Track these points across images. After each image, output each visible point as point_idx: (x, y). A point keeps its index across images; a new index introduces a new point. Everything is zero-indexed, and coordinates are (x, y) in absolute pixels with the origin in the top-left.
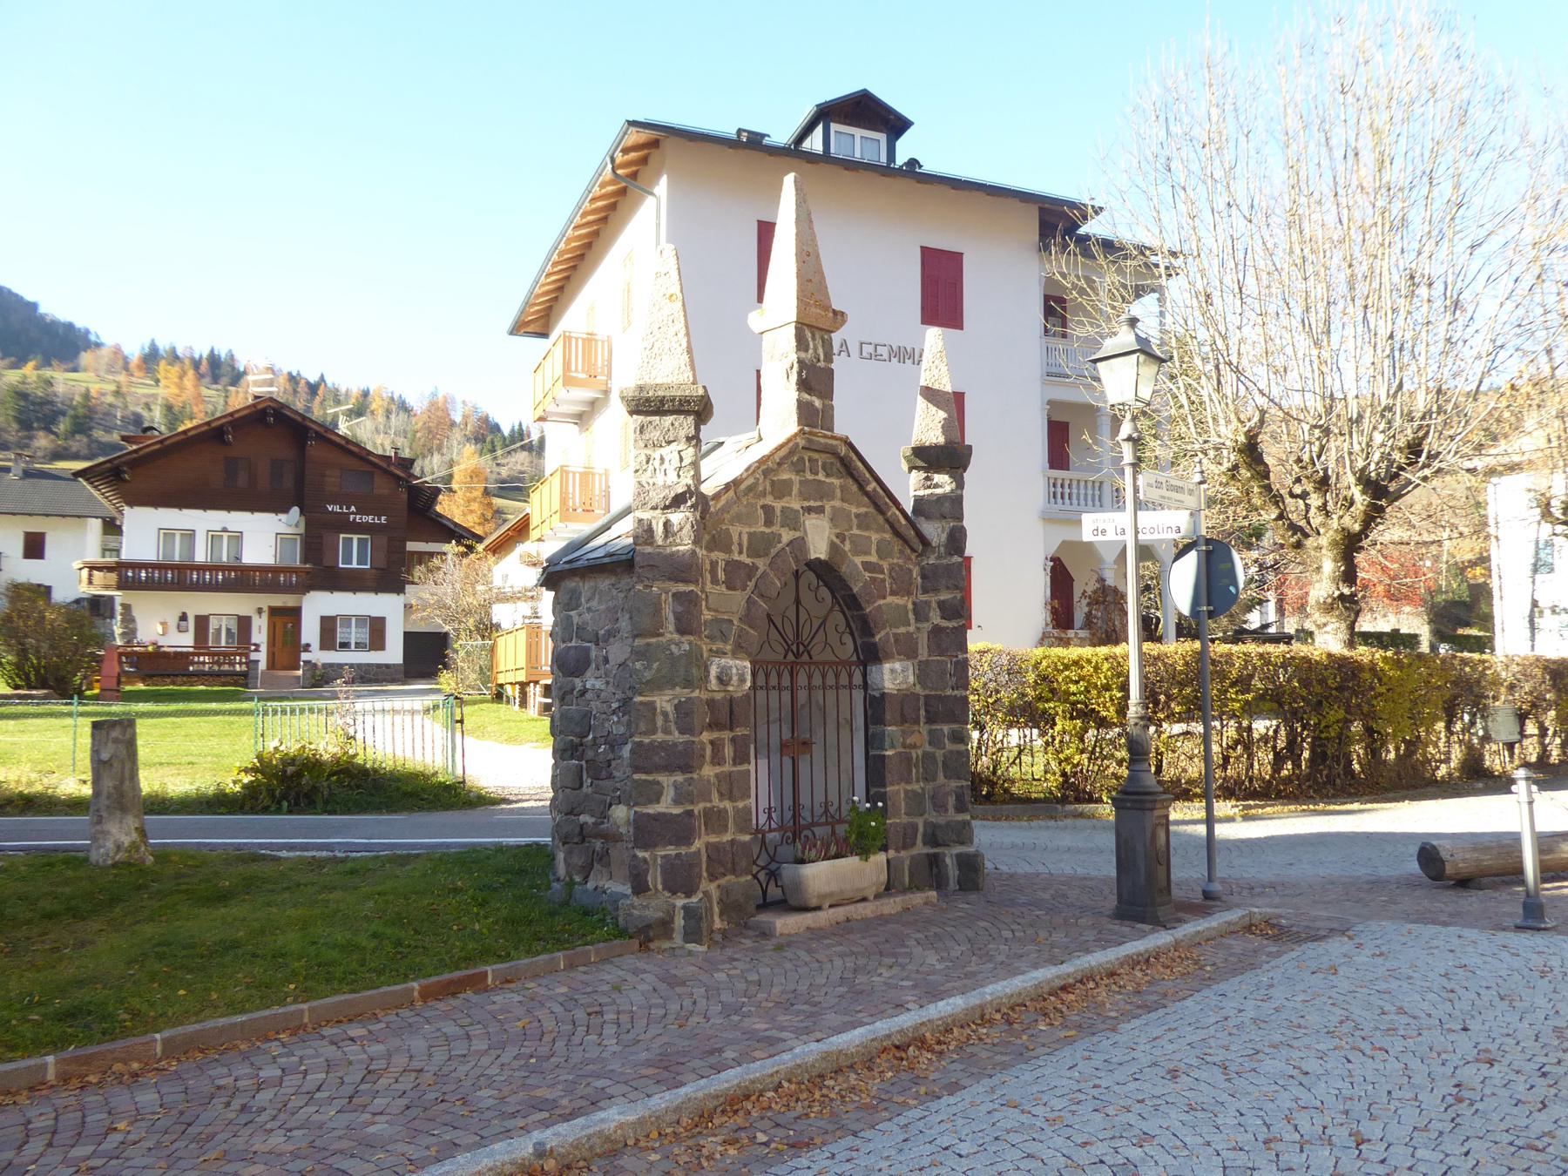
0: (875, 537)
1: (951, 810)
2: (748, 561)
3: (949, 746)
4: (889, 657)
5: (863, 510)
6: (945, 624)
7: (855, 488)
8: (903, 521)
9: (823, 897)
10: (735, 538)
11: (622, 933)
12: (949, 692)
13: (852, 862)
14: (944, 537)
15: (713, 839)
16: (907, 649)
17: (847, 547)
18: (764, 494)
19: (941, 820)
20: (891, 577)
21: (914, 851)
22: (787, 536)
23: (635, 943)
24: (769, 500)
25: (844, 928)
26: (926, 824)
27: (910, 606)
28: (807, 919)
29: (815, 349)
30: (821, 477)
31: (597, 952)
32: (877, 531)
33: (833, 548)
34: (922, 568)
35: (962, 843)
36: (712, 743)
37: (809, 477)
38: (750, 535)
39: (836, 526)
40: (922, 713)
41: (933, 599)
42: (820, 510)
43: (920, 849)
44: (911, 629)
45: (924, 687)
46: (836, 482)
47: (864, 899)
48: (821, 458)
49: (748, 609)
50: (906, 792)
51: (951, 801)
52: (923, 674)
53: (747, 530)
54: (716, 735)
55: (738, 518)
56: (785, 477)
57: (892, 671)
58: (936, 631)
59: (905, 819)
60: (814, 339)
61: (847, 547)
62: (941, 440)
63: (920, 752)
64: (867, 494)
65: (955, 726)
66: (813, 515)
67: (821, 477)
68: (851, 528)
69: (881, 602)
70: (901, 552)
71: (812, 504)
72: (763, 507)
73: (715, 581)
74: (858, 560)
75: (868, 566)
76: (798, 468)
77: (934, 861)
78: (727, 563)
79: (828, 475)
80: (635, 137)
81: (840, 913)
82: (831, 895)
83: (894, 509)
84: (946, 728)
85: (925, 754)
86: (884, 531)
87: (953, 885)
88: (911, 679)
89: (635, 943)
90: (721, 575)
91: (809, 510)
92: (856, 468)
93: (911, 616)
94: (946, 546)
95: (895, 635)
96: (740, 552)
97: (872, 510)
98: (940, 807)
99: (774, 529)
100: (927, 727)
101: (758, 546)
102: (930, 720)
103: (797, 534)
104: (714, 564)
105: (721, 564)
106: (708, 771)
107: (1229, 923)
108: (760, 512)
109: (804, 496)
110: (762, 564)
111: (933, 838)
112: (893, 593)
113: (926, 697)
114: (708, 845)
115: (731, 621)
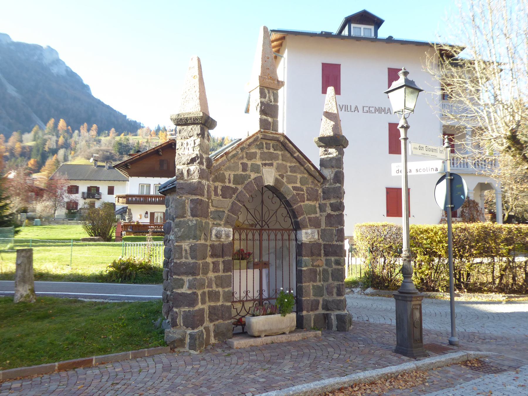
0: (299, 176)
1: (335, 295)
2: (234, 186)
3: (334, 266)
4: (305, 227)
5: (293, 164)
6: (333, 213)
7: (289, 155)
8: (313, 169)
9: (261, 332)
10: (227, 177)
11: (165, 344)
12: (335, 243)
13: (277, 317)
14: (333, 175)
15: (212, 304)
16: (315, 223)
17: (285, 180)
18: (242, 158)
19: (330, 299)
20: (307, 193)
21: (317, 312)
22: (253, 176)
23: (168, 348)
24: (245, 161)
25: (267, 346)
26: (324, 300)
27: (317, 205)
29: (269, 97)
30: (272, 150)
31: (148, 352)
32: (300, 173)
33: (277, 180)
34: (323, 189)
35: (339, 310)
36: (213, 263)
37: (265, 150)
38: (234, 175)
39: (279, 171)
40: (322, 252)
41: (328, 202)
42: (271, 165)
43: (321, 311)
44: (318, 215)
45: (323, 240)
46: (280, 153)
47: (284, 333)
48: (272, 143)
49: (232, 206)
50: (313, 286)
51: (335, 290)
52: (323, 234)
53: (234, 173)
54: (215, 259)
55: (229, 168)
56: (253, 151)
57: (306, 233)
58: (329, 216)
59: (312, 298)
60: (269, 93)
61: (285, 180)
62: (332, 134)
63: (321, 269)
64: (295, 158)
65: (337, 258)
66: (267, 167)
67: (272, 150)
68: (287, 172)
69: (302, 204)
70: (312, 182)
71: (267, 162)
72: (241, 163)
73: (216, 194)
74: (290, 186)
75: (295, 188)
76: (260, 147)
77: (326, 317)
78: (223, 187)
79: (275, 150)
81: (269, 339)
82: (265, 331)
83: (308, 164)
84: (333, 259)
85: (324, 270)
86: (303, 173)
87: (334, 328)
88: (316, 237)
89: (168, 348)
90: (219, 192)
91: (265, 165)
92: (289, 147)
93: (318, 210)
94: (333, 179)
95: (309, 218)
96: (230, 182)
97: (298, 164)
98: (330, 293)
99: (247, 173)
100: (325, 258)
101: (238, 180)
102: (326, 255)
103: (259, 175)
104: (216, 188)
105: (219, 188)
106: (211, 275)
107: (453, 359)
108: (240, 166)
109: (262, 158)
110: (240, 187)
111: (326, 307)
112: (308, 200)
113: (324, 245)
114: (210, 307)
115: (224, 212)
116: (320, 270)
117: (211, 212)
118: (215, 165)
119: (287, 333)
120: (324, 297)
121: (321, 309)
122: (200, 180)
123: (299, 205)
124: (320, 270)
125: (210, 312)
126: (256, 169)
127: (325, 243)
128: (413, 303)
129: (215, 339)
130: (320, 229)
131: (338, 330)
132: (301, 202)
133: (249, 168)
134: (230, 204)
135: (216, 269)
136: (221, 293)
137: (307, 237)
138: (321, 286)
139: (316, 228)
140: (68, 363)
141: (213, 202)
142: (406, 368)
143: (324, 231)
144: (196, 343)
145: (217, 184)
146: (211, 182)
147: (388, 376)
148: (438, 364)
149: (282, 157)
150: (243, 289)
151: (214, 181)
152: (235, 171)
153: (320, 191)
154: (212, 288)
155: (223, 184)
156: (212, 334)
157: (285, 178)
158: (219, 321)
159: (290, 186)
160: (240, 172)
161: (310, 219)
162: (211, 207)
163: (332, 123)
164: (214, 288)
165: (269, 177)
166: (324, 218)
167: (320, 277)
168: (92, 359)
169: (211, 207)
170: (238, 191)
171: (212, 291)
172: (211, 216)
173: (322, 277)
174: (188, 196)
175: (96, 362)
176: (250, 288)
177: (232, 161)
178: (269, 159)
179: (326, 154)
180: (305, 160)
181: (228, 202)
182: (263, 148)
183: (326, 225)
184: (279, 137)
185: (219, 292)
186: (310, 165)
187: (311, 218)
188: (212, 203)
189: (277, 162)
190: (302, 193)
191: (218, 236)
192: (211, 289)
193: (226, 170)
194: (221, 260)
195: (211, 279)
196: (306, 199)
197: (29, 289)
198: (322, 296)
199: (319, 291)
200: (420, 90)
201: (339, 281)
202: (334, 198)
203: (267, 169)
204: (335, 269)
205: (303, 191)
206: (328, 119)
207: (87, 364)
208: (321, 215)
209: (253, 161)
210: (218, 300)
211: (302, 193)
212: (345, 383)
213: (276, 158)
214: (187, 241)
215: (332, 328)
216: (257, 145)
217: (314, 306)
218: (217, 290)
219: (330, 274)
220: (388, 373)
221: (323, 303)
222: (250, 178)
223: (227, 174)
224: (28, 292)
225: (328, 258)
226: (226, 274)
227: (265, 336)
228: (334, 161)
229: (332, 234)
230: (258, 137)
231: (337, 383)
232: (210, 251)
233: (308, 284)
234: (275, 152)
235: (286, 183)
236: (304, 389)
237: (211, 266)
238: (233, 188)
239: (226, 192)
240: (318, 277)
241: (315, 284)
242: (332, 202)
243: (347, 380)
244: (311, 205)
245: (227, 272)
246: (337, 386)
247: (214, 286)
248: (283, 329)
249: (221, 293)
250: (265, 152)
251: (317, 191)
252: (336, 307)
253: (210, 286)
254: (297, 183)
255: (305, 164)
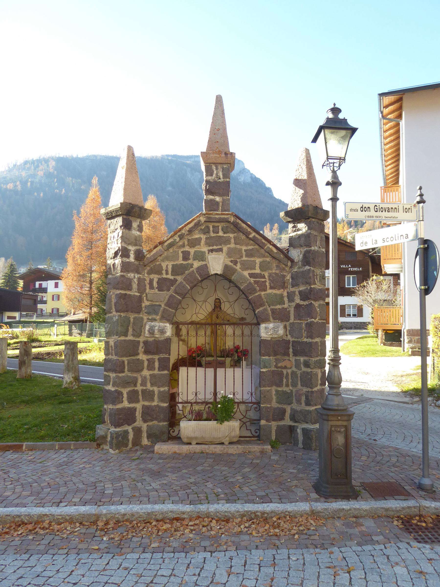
0: (258, 261)
1: (303, 404)
2: (172, 278)
3: (304, 369)
4: (266, 320)
5: (250, 247)
6: (302, 303)
7: (243, 237)
8: (275, 250)
9: (192, 438)
10: (164, 268)
11: (93, 440)
12: (305, 340)
13: (212, 424)
14: (301, 256)
15: (146, 403)
16: (281, 316)
17: (238, 267)
18: (183, 246)
19: (298, 408)
20: (269, 280)
21: (282, 423)
22: (196, 264)
23: (95, 444)
24: (187, 249)
25: (190, 456)
26: (292, 409)
27: (285, 294)
28: (185, 449)
29: (217, 174)
30: (221, 234)
31: (74, 445)
32: (259, 257)
33: (226, 267)
34: (292, 274)
35: (307, 423)
36: (148, 360)
37: (212, 235)
38: (173, 265)
39: (230, 257)
40: (291, 350)
41: (296, 290)
42: (221, 250)
43: (287, 422)
44: (286, 306)
45: (292, 336)
46: (232, 235)
47: (223, 443)
48: (221, 225)
49: (169, 300)
50: (277, 391)
51: (303, 398)
52: (292, 329)
53: (172, 263)
54: (150, 357)
55: (167, 259)
56: (197, 236)
57: (266, 328)
58: (298, 306)
59: (274, 404)
60: (217, 169)
61: (238, 267)
62: (300, 205)
63: (289, 371)
64: (250, 239)
65: (306, 358)
66: (214, 253)
67: (221, 234)
68: (242, 257)
69: (263, 293)
70: (277, 266)
71: (215, 247)
72: (182, 252)
73: (151, 287)
74: (246, 273)
75: (251, 275)
76: (206, 231)
77: (292, 429)
78: (159, 279)
79: (224, 233)
80: (387, 100)
81: (199, 448)
82: (196, 438)
83: (269, 245)
84: (302, 359)
85: (293, 373)
86: (264, 256)
87: (301, 445)
88: (281, 332)
89: (95, 444)
90: (155, 285)
91: (212, 251)
92: (242, 228)
93: (286, 299)
94: (302, 261)
95: (272, 310)
96: (167, 273)
97: (257, 247)
98: (299, 402)
99: (190, 262)
100: (294, 358)
101: (177, 270)
102: (295, 354)
103: (204, 263)
104: (151, 281)
105: (155, 281)
106: (146, 373)
107: (387, 510)
108: (181, 255)
109: (208, 244)
110: (180, 278)
111: (293, 418)
112: (271, 288)
113: (293, 341)
114: (143, 406)
115: (160, 305)
116: (287, 373)
117: (146, 307)
118: (148, 256)
119: (227, 443)
120: (292, 405)
121: (289, 420)
122: (122, 274)
123: (257, 294)
124: (287, 373)
125: (142, 411)
126: (200, 256)
127: (294, 339)
128: (331, 423)
129: (148, 441)
130: (288, 324)
131: (303, 448)
132: (261, 290)
133: (191, 257)
134: (167, 297)
135: (151, 367)
136: (156, 393)
137: (268, 332)
138: (289, 391)
139: (282, 320)
140: (3, 445)
141: (148, 296)
142: (290, 509)
143: (292, 325)
144: (120, 442)
145: (152, 276)
146: (146, 275)
147: (256, 515)
148: (356, 513)
149: (235, 240)
150: (192, 389)
151: (149, 273)
152: (174, 261)
153: (288, 277)
154: (146, 386)
155: (159, 276)
156: (145, 435)
157: (239, 265)
158: (154, 422)
159: (246, 273)
160: (180, 261)
161: (273, 311)
162: (146, 302)
163: (302, 191)
164: (149, 386)
165: (216, 264)
166: (293, 309)
167: (287, 381)
168: (23, 445)
169: (146, 302)
170: (178, 283)
171: (146, 390)
172: (146, 311)
173: (290, 381)
174: (114, 291)
175: (26, 448)
176: (201, 388)
177: (171, 250)
178: (216, 244)
179: (295, 231)
180: (264, 241)
181: (165, 295)
182: (208, 232)
183: (295, 318)
184: (228, 218)
185: (153, 391)
186: (271, 247)
187: (276, 309)
188: (146, 297)
189: (228, 246)
190: (263, 280)
191: (151, 331)
192: (144, 388)
193: (163, 261)
194: (156, 357)
195: (145, 377)
196: (268, 287)
197: (72, 377)
198: (289, 404)
199: (285, 398)
200: (354, 130)
201: (308, 387)
202: (303, 284)
203: (213, 256)
204: (304, 372)
205: (264, 277)
206: (297, 188)
207: (17, 448)
208: (289, 306)
209: (197, 248)
210: (153, 400)
211: (263, 280)
212: (183, 513)
213: (227, 241)
214: (113, 337)
215: (298, 443)
216: (201, 229)
217: (280, 415)
218: (151, 389)
219: (299, 378)
220: (257, 512)
221: (291, 413)
222: (192, 267)
223: (164, 265)
224: (72, 379)
225: (297, 358)
226: (162, 372)
227: (197, 444)
228: (303, 239)
229: (301, 329)
230: (199, 221)
231: (171, 512)
232: (142, 347)
233: (270, 388)
234: (225, 235)
235: (240, 270)
236: (123, 511)
237: (146, 363)
238: (171, 279)
239: (163, 284)
240: (285, 380)
241: (280, 389)
242: (301, 289)
243: (188, 510)
244: (275, 294)
245: (162, 371)
246: (171, 515)
247: (149, 384)
248: (220, 438)
249: (156, 393)
250: (212, 237)
251: (284, 276)
252: (303, 419)
253: (144, 383)
254: (255, 269)
255: (265, 245)
